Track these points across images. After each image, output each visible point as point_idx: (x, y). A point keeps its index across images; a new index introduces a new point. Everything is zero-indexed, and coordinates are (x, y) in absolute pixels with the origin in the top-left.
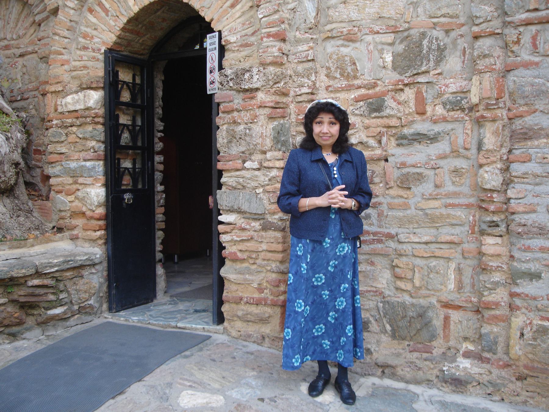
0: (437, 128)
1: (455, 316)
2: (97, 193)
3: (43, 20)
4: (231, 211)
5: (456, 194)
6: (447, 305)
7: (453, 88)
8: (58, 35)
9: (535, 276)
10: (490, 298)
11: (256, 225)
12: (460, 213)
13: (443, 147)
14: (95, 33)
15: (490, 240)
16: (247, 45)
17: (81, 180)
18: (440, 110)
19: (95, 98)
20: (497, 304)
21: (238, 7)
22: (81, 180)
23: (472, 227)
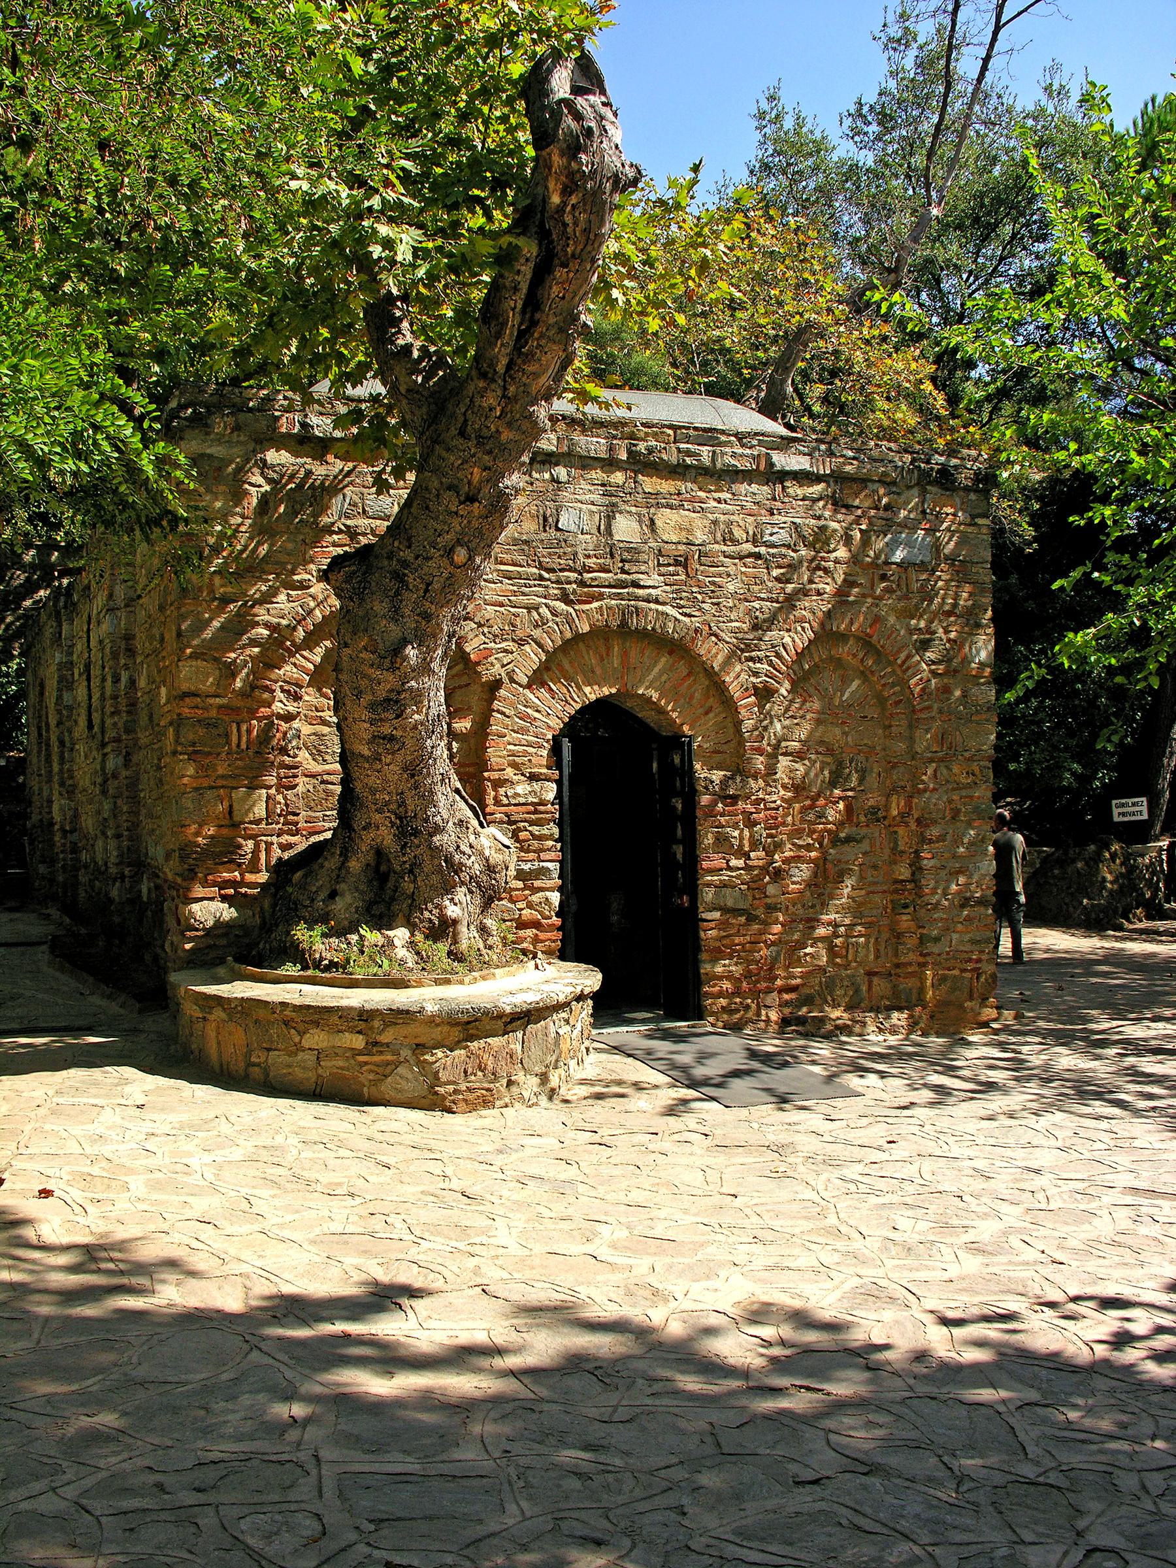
0: (864, 831)
1: (875, 980)
2: (555, 898)
3: (460, 687)
4: (715, 909)
5: (875, 883)
6: (870, 974)
7: (871, 802)
8: (503, 713)
9: (937, 940)
10: (903, 959)
11: (743, 919)
12: (877, 898)
13: (865, 846)
14: (537, 715)
15: (904, 918)
16: (719, 752)
17: (537, 883)
18: (863, 819)
19: (550, 791)
20: (910, 964)
21: (711, 715)
22: (537, 883)
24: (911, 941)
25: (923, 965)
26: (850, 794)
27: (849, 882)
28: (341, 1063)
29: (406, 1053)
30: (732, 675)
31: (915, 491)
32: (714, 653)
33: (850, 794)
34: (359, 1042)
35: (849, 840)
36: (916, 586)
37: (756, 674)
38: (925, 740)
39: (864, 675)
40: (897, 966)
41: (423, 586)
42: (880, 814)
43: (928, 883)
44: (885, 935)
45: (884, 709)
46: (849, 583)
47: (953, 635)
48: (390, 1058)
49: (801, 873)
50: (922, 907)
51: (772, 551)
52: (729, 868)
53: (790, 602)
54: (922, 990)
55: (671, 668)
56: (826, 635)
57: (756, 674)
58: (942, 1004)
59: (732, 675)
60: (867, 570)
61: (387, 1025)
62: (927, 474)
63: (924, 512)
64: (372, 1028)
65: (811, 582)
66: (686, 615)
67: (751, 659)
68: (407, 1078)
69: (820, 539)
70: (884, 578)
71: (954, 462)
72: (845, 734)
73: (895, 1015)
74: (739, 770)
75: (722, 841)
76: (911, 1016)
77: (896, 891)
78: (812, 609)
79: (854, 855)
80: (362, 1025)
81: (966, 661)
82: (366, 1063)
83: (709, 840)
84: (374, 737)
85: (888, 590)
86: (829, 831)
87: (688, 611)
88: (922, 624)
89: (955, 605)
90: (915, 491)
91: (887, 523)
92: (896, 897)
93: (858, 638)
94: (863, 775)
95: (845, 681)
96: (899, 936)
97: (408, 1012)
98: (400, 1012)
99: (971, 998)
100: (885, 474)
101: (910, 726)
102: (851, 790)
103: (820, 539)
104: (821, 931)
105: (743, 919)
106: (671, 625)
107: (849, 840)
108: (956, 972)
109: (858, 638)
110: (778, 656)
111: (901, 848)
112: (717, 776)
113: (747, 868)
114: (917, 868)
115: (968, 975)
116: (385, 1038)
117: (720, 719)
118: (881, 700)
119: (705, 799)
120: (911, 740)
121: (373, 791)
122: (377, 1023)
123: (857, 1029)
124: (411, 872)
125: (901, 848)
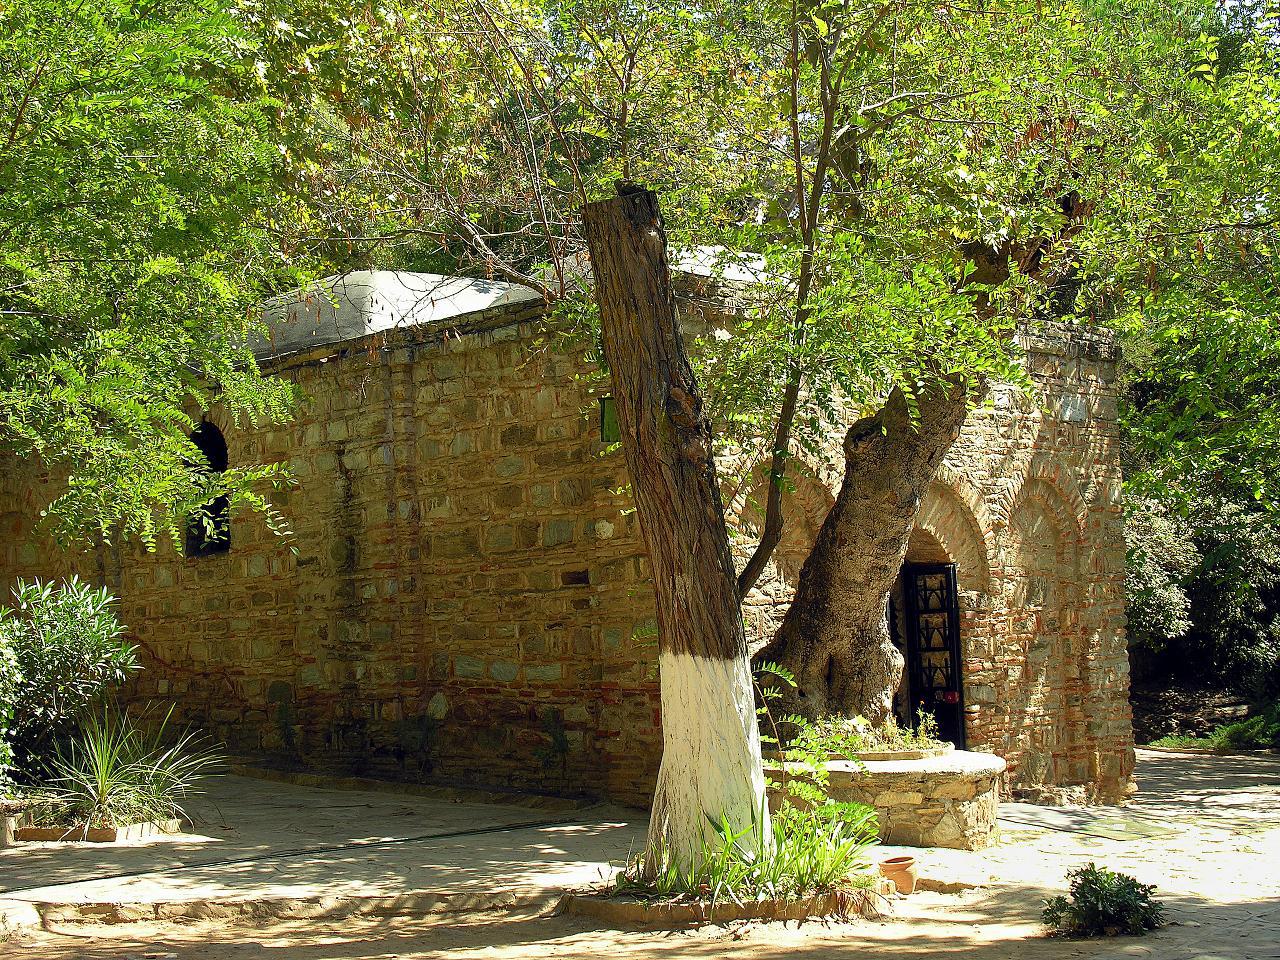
10: (1078, 743)
13: (1048, 650)
23: (1061, 702)
24: (1081, 729)
25: (1093, 747)
26: (1040, 608)
27: (1041, 680)
28: (904, 817)
29: (948, 805)
30: (981, 513)
31: (1074, 363)
32: (969, 495)
33: (1040, 608)
34: (917, 798)
35: (1040, 646)
36: (1078, 439)
37: (993, 512)
38: (1087, 563)
39: (1046, 510)
40: (1074, 749)
41: (929, 454)
42: (1057, 624)
43: (1093, 679)
44: (1062, 724)
45: (1056, 539)
46: (1041, 438)
47: (1100, 479)
48: (939, 810)
49: (1015, 673)
50: (1089, 700)
51: (1000, 413)
52: (984, 669)
53: (1009, 454)
54: (1092, 767)
55: (941, 509)
56: (1031, 482)
57: (993, 512)
58: (1106, 779)
59: (981, 513)
60: (1053, 424)
61: (938, 784)
62: (1082, 348)
63: (1079, 379)
64: (927, 788)
65: (1021, 438)
66: (954, 465)
67: (990, 501)
68: (948, 828)
69: (1023, 405)
70: (1060, 433)
71: (1095, 338)
72: (1035, 559)
73: (1077, 789)
74: (986, 590)
75: (979, 646)
76: (1087, 790)
77: (1070, 688)
78: (1023, 457)
79: (1041, 655)
80: (921, 786)
81: (1108, 499)
82: (923, 815)
83: (971, 647)
84: (873, 568)
85: (1063, 443)
86: (1029, 639)
87: (956, 462)
88: (1083, 471)
89: (1100, 454)
90: (1074, 363)
91: (1060, 391)
92: (1069, 692)
93: (1044, 483)
94: (1045, 590)
95: (1034, 517)
96: (1074, 724)
97: (954, 773)
98: (949, 773)
99: (1121, 775)
100: (1060, 349)
101: (1076, 553)
102: (1040, 605)
103: (1023, 405)
104: (1027, 721)
105: (993, 710)
106: (946, 473)
107: (1040, 646)
108: (1112, 753)
109: (1044, 483)
110: (1005, 497)
111: (1072, 652)
112: (973, 594)
113: (994, 669)
114: (1084, 668)
115: (1119, 755)
116: (935, 795)
117: (970, 549)
118: (1056, 532)
119: (969, 614)
120: (1078, 564)
121: (849, 609)
122: (930, 784)
123: (1058, 801)
124: (860, 673)
125: (1072, 652)
